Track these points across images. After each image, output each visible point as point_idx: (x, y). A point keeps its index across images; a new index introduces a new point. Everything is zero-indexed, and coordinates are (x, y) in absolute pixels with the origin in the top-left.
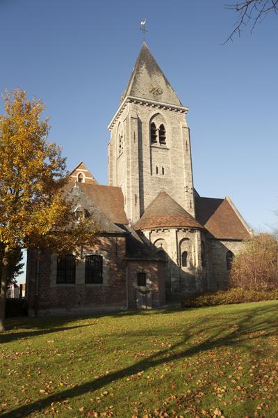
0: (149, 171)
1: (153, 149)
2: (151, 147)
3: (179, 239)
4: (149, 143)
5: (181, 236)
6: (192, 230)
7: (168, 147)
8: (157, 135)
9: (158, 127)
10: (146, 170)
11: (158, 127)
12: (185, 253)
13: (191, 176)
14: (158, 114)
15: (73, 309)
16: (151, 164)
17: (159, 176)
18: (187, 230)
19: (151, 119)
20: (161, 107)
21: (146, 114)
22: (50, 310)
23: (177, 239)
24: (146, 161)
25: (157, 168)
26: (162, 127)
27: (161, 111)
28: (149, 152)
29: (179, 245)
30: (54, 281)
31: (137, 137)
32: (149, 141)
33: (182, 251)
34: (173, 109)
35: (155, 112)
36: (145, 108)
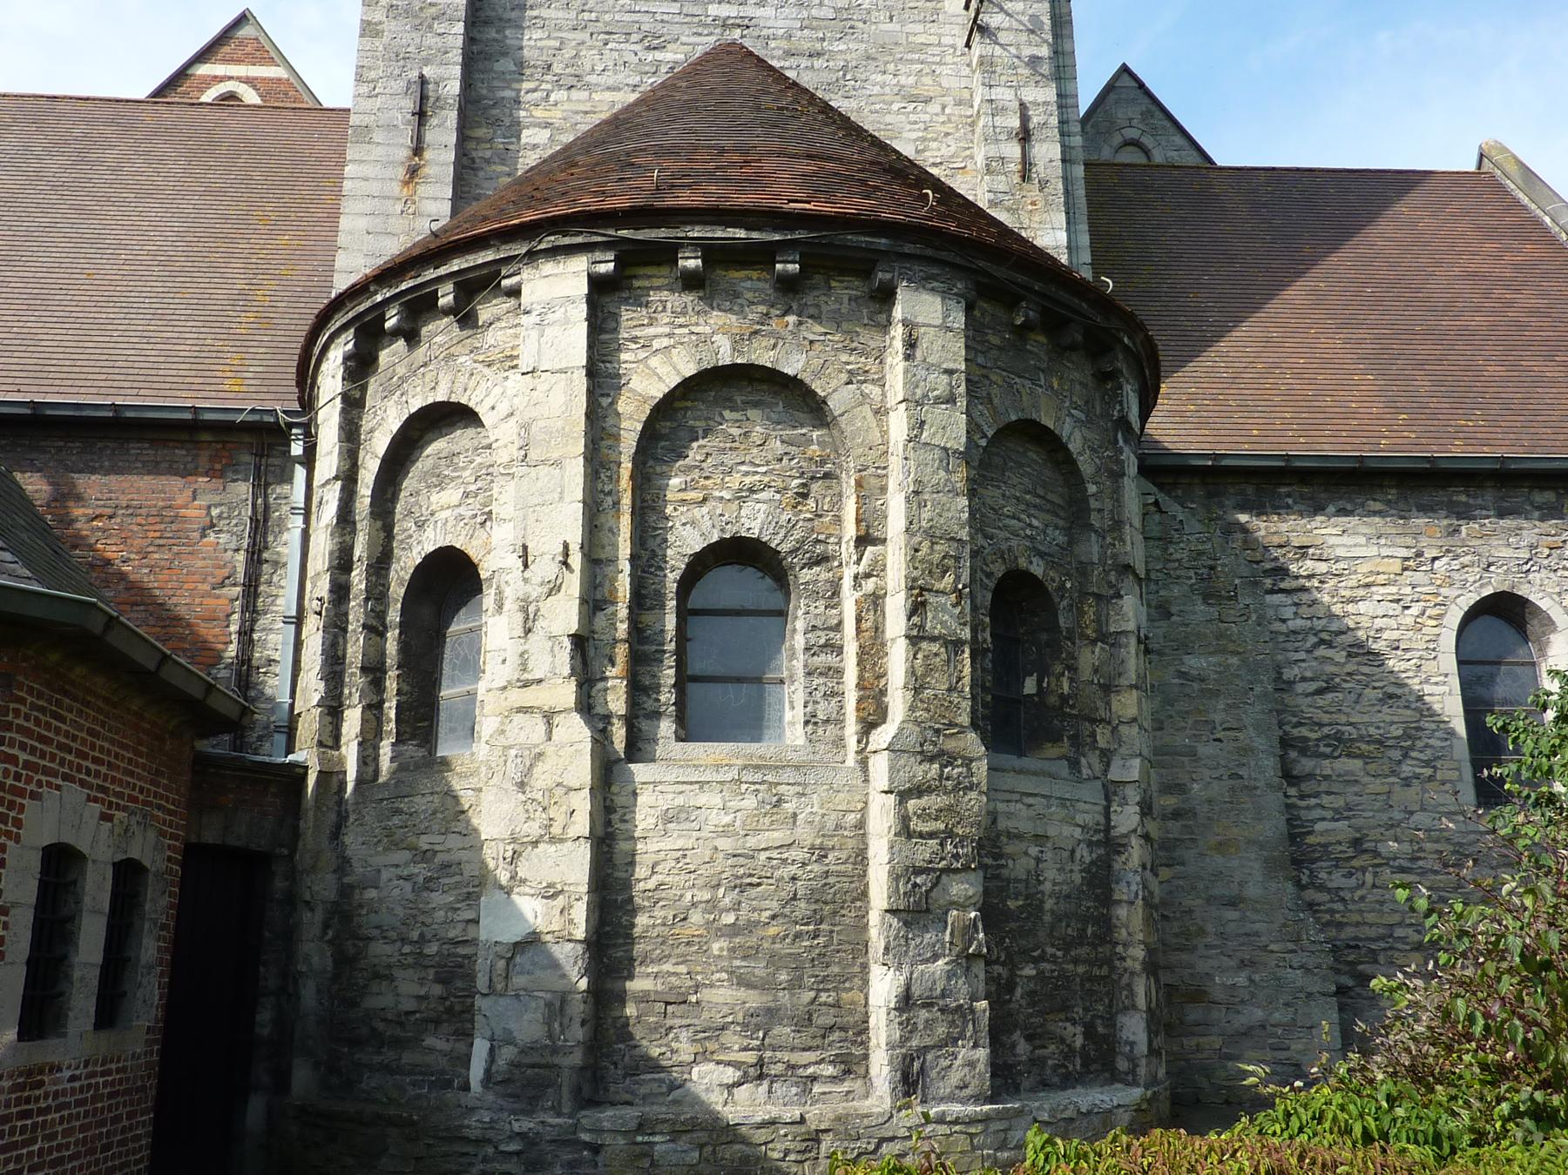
23: (601, 376)
29: (635, 458)
33: (688, 535)
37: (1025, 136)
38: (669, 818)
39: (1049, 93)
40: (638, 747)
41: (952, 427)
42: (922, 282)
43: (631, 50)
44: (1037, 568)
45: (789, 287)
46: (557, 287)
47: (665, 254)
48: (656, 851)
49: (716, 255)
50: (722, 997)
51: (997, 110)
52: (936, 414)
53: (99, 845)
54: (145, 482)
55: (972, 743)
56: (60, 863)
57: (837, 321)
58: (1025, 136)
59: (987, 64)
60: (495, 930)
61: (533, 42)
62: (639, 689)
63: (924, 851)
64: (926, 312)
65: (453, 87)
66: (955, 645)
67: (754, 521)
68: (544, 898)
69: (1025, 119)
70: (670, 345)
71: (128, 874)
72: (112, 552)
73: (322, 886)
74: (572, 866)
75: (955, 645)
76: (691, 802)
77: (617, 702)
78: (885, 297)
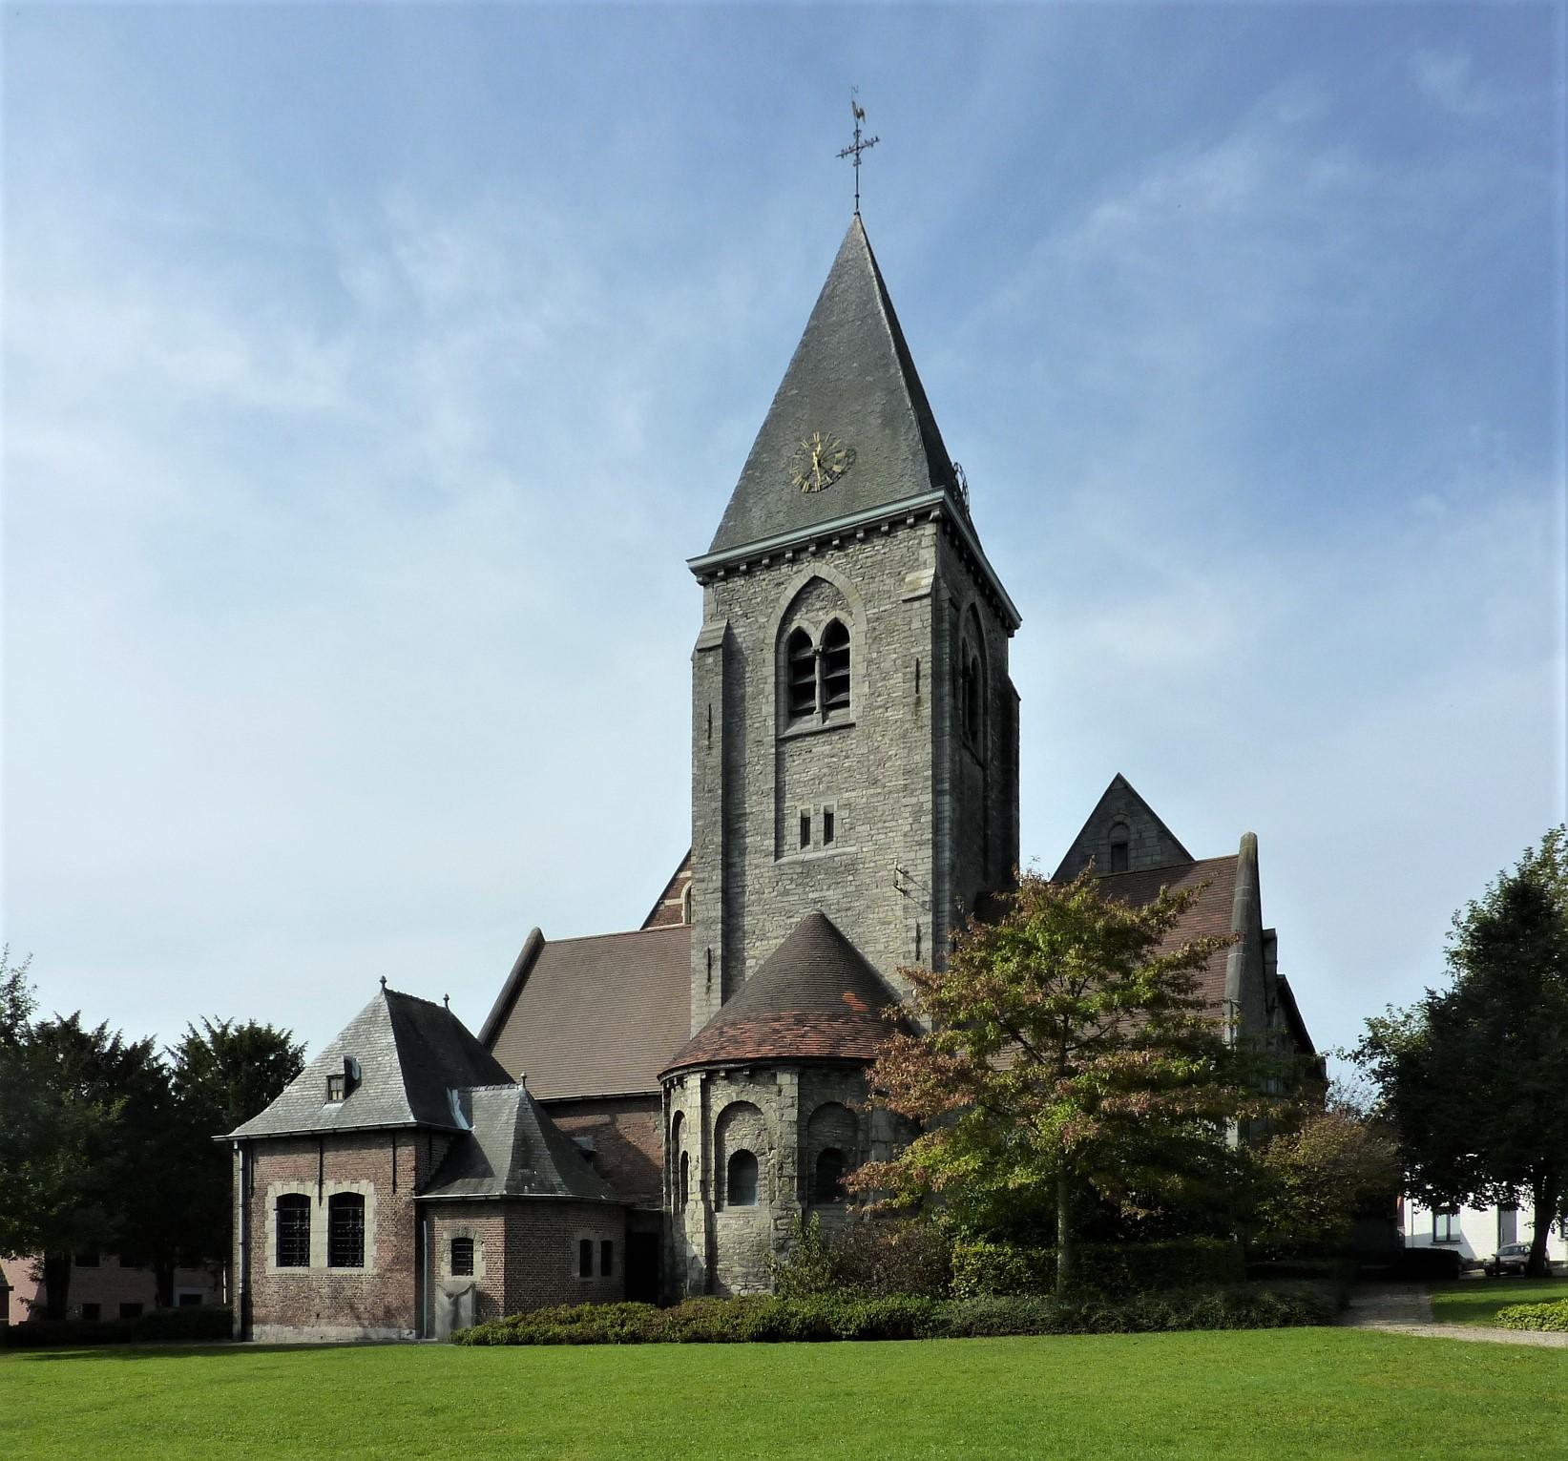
0: (770, 843)
1: (790, 747)
2: (780, 742)
3: (718, 1106)
4: (772, 732)
5: (722, 1096)
6: (759, 1070)
7: (852, 719)
8: (815, 673)
9: (816, 639)
10: (757, 839)
11: (816, 639)
12: (744, 1160)
13: (927, 819)
14: (815, 581)
15: (306, 1329)
16: (778, 810)
17: (810, 854)
18: (740, 1070)
19: (787, 619)
20: (823, 544)
21: (762, 612)
22: (267, 1328)
23: (705, 1107)
24: (758, 807)
25: (805, 822)
26: (837, 633)
27: (822, 568)
28: (771, 769)
29: (715, 1129)
30: (272, 1260)
31: (718, 723)
32: (771, 722)
33: (730, 1150)
34: (871, 530)
35: (799, 582)
36: (764, 579)
37: (918, 940)
38: (725, 1226)
39: (929, 918)
40: (719, 1208)
41: (793, 1114)
42: (784, 1071)
43: (781, 920)
44: (838, 1146)
45: (751, 1078)
46: (694, 1082)
47: (717, 1071)
48: (722, 1235)
49: (729, 1072)
50: (737, 1269)
51: (908, 929)
52: (786, 1112)
53: (596, 1238)
54: (637, 1115)
55: (797, 1205)
56: (586, 1245)
57: (764, 1085)
58: (918, 940)
59: (905, 908)
60: (689, 1254)
61: (748, 921)
62: (719, 1193)
63: (782, 1234)
64: (787, 1081)
65: (719, 952)
66: (792, 1178)
67: (746, 1145)
68: (696, 1247)
69: (918, 931)
70: (722, 1096)
71: (606, 1246)
72: (631, 1139)
73: (667, 1242)
74: (701, 1238)
75: (792, 1178)
76: (731, 1222)
77: (712, 1197)
78: (775, 1076)
